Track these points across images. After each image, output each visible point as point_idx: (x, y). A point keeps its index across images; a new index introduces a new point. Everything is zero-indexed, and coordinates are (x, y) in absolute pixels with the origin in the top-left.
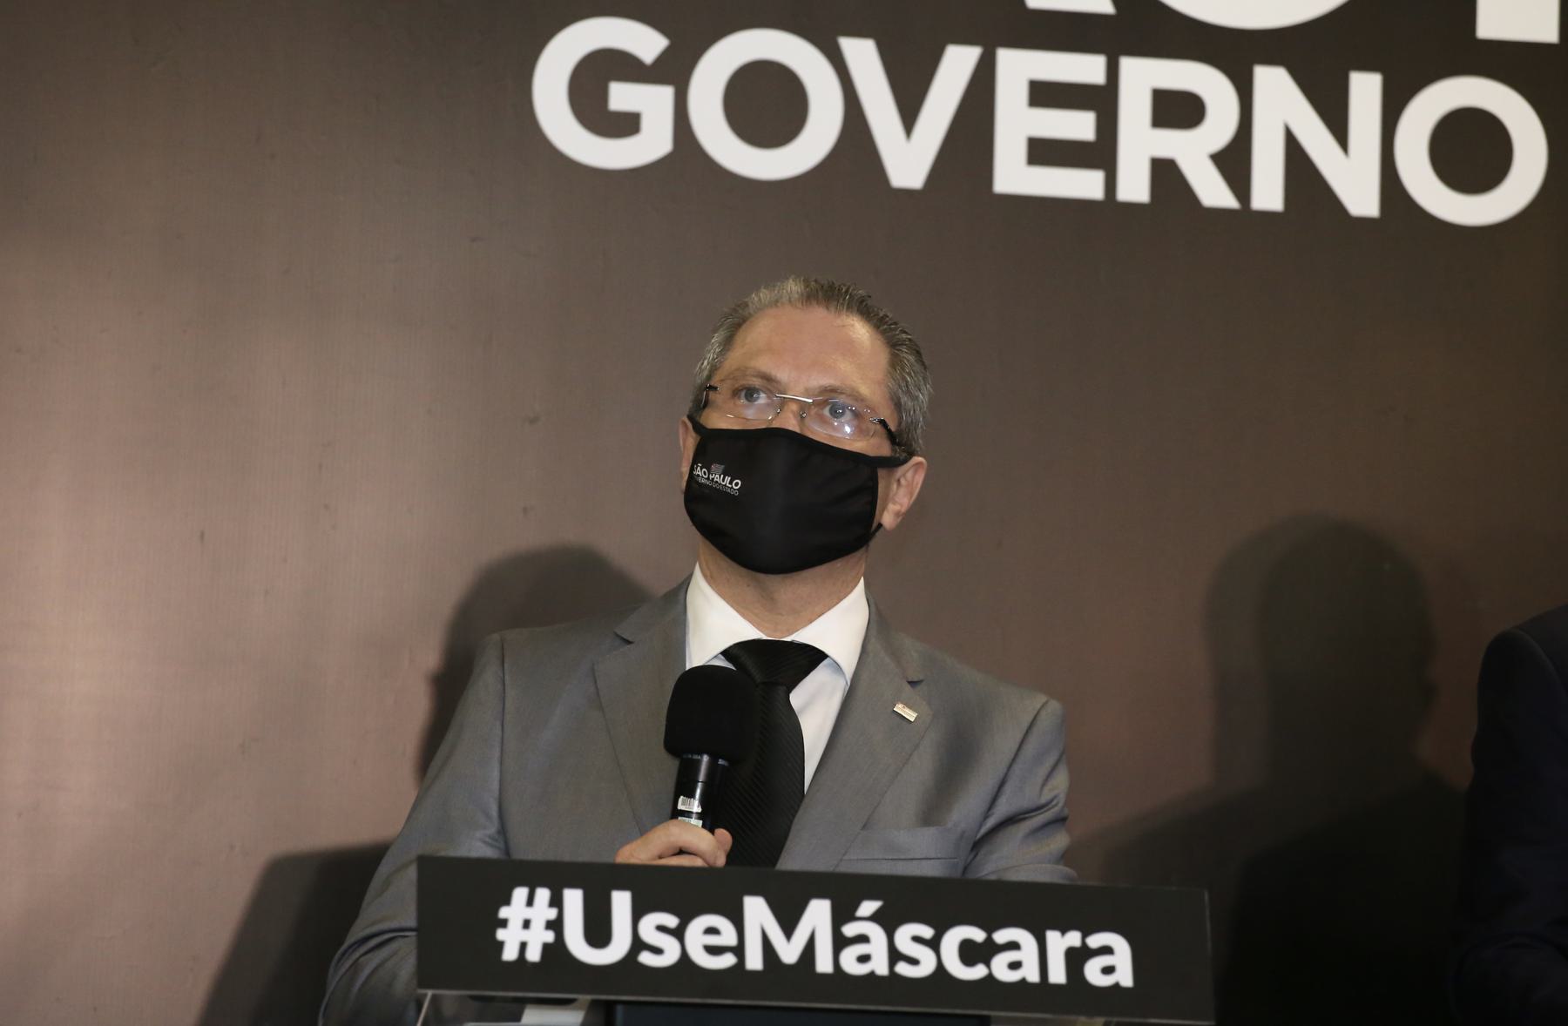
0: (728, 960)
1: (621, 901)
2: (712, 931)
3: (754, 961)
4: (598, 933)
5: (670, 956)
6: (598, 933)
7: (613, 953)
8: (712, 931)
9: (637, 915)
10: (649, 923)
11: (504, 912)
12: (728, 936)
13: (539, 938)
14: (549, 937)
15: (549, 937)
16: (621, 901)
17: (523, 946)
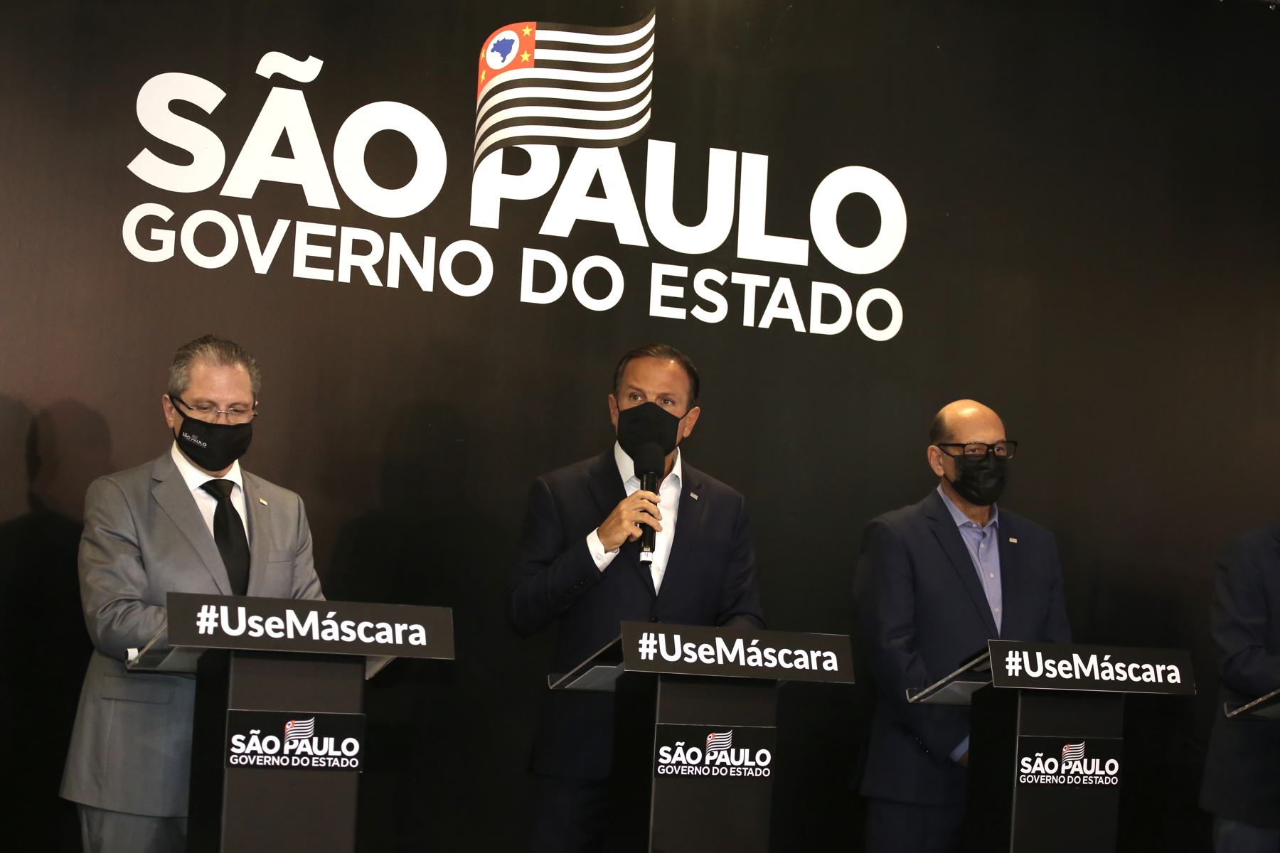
0: (281, 635)
1: (242, 611)
2: (275, 623)
3: (291, 635)
4: (234, 623)
5: (260, 633)
6: (234, 623)
7: (239, 631)
8: (275, 623)
9: (248, 616)
10: (253, 619)
11: (199, 615)
12: (281, 625)
13: (212, 625)
14: (216, 625)
15: (216, 625)
16: (242, 611)
17: (207, 628)
